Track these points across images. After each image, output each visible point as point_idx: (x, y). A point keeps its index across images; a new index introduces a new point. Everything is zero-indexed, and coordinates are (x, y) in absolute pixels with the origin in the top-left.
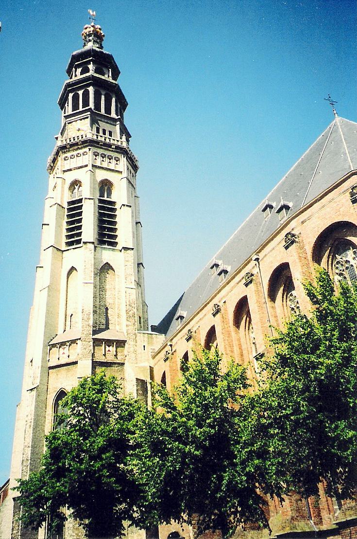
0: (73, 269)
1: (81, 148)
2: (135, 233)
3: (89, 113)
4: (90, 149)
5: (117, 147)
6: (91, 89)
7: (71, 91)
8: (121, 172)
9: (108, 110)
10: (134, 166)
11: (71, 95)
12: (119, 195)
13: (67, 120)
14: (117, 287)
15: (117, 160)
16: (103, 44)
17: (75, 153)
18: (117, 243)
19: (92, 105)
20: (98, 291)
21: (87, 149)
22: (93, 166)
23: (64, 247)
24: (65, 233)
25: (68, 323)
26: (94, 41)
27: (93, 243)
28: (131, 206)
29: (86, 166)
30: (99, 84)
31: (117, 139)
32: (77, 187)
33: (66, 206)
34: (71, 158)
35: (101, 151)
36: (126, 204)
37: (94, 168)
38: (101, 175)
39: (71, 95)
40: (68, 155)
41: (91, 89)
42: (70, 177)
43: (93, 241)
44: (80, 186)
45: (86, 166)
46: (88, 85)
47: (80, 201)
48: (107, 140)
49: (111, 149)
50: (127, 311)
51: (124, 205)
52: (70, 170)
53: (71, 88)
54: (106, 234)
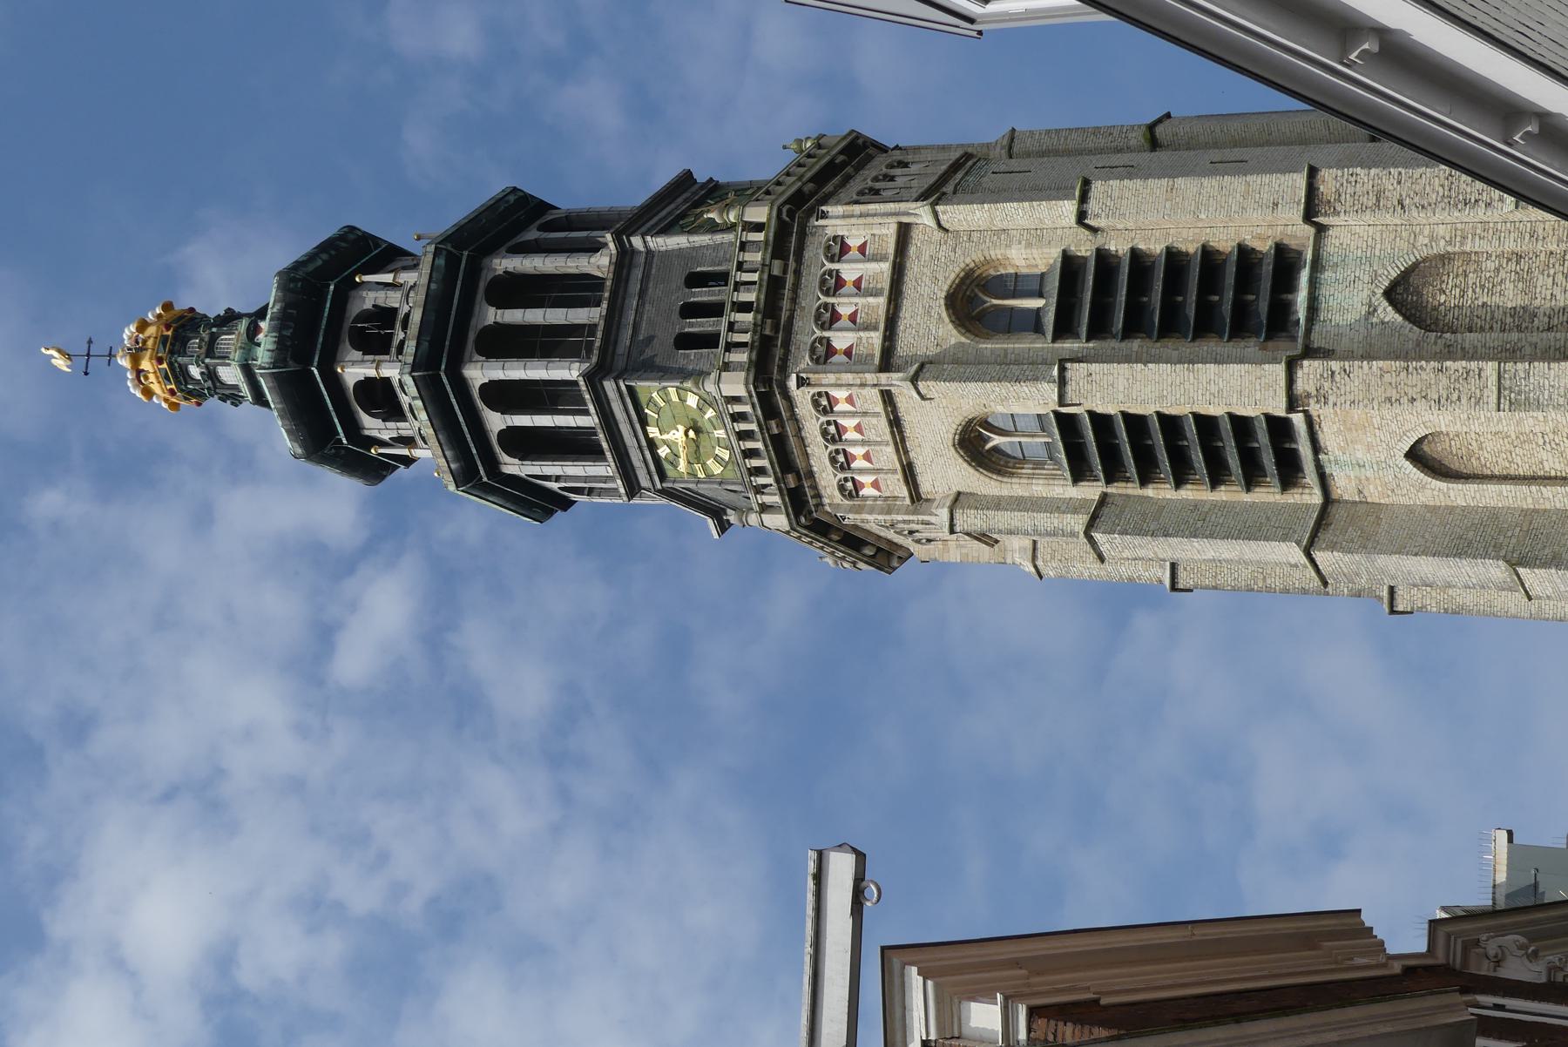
0: (1415, 455)
2: (1216, 155)
3: (609, 386)
4: (801, 382)
5: (779, 248)
6: (479, 374)
7: (493, 465)
8: (904, 232)
9: (578, 290)
10: (847, 164)
11: (512, 466)
12: (1028, 236)
13: (644, 482)
14: (1510, 245)
15: (838, 250)
16: (215, 310)
19: (568, 371)
20: (1535, 338)
21: (802, 398)
22: (886, 365)
26: (210, 353)
27: (1291, 367)
28: (1086, 183)
29: (888, 398)
31: (734, 240)
32: (997, 440)
33: (1091, 491)
34: (846, 467)
35: (806, 332)
36: (1069, 208)
37: (896, 361)
38: (928, 326)
39: (512, 466)
42: (945, 472)
44: (986, 424)
45: (888, 398)
46: (461, 385)
47: (1067, 424)
48: (749, 296)
49: (790, 278)
51: (1081, 217)
52: (909, 474)
53: (475, 468)
54: (1240, 299)
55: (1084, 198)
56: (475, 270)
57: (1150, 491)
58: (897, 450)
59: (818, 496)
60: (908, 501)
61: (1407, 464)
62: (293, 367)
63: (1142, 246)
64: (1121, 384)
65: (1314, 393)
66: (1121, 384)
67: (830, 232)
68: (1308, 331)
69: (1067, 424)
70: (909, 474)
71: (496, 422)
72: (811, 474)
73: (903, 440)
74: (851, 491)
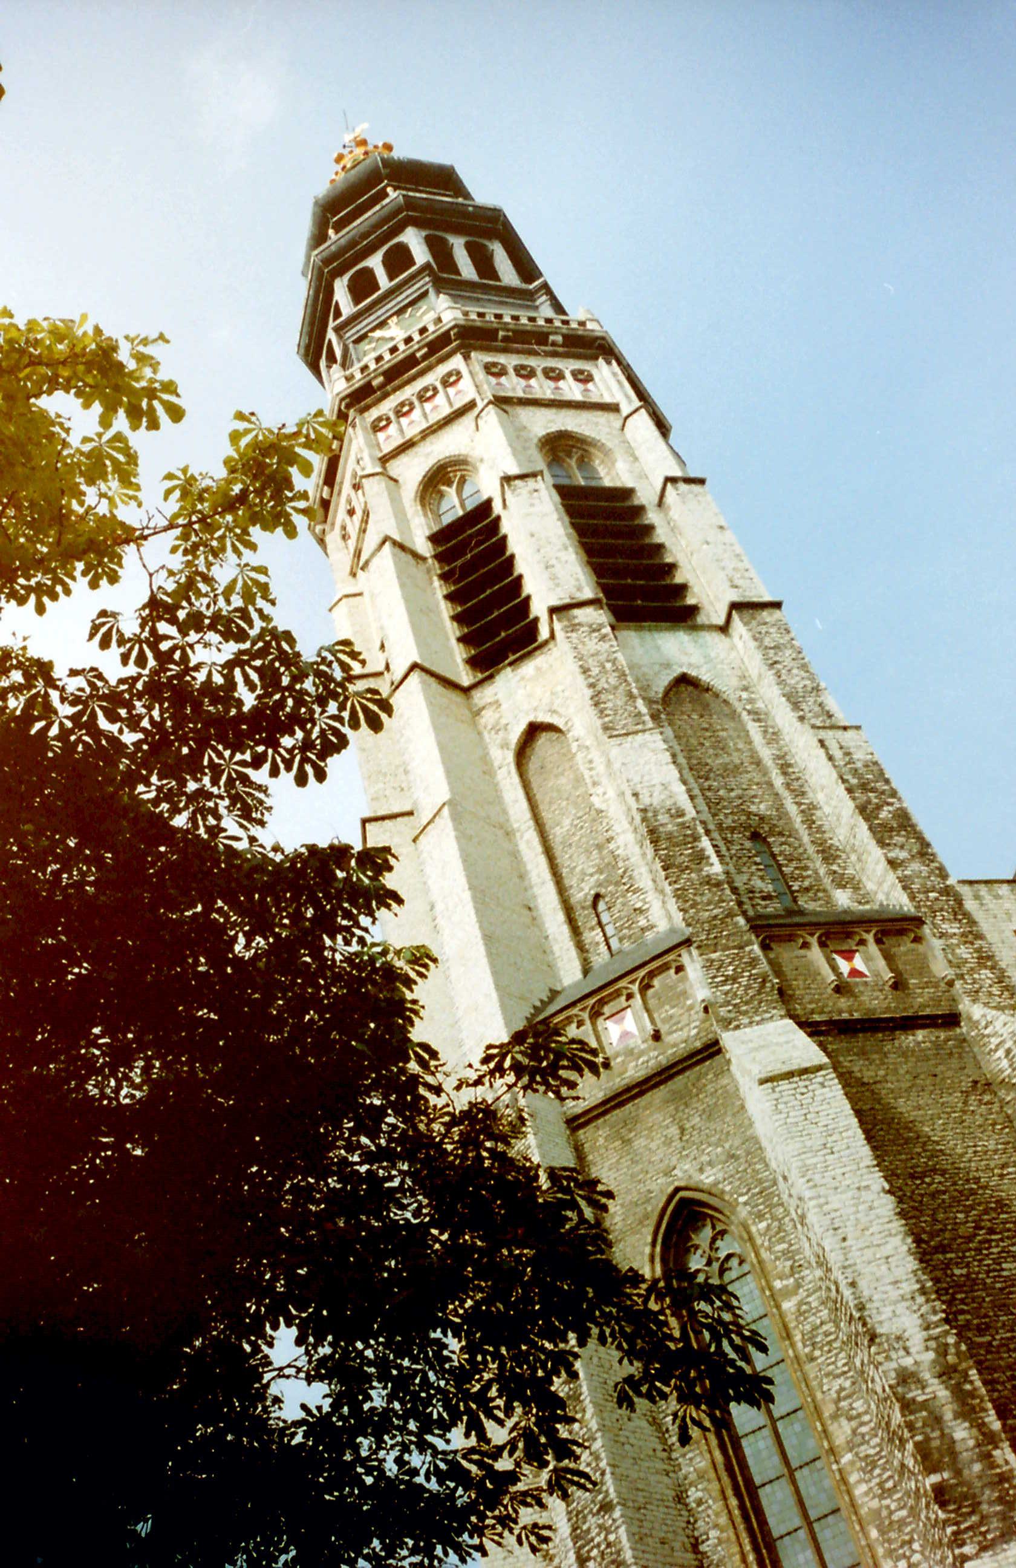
4: (467, 357)
7: (339, 272)
8: (614, 408)
23: (466, 677)
24: (453, 631)
25: (593, 936)
35: (509, 361)
40: (387, 407)
41: (413, 240)
44: (463, 481)
46: (399, 229)
52: (407, 446)
57: (437, 583)
58: (423, 431)
60: (380, 455)
65: (576, 621)
67: (595, 372)
70: (407, 446)
72: (386, 395)
73: (434, 432)
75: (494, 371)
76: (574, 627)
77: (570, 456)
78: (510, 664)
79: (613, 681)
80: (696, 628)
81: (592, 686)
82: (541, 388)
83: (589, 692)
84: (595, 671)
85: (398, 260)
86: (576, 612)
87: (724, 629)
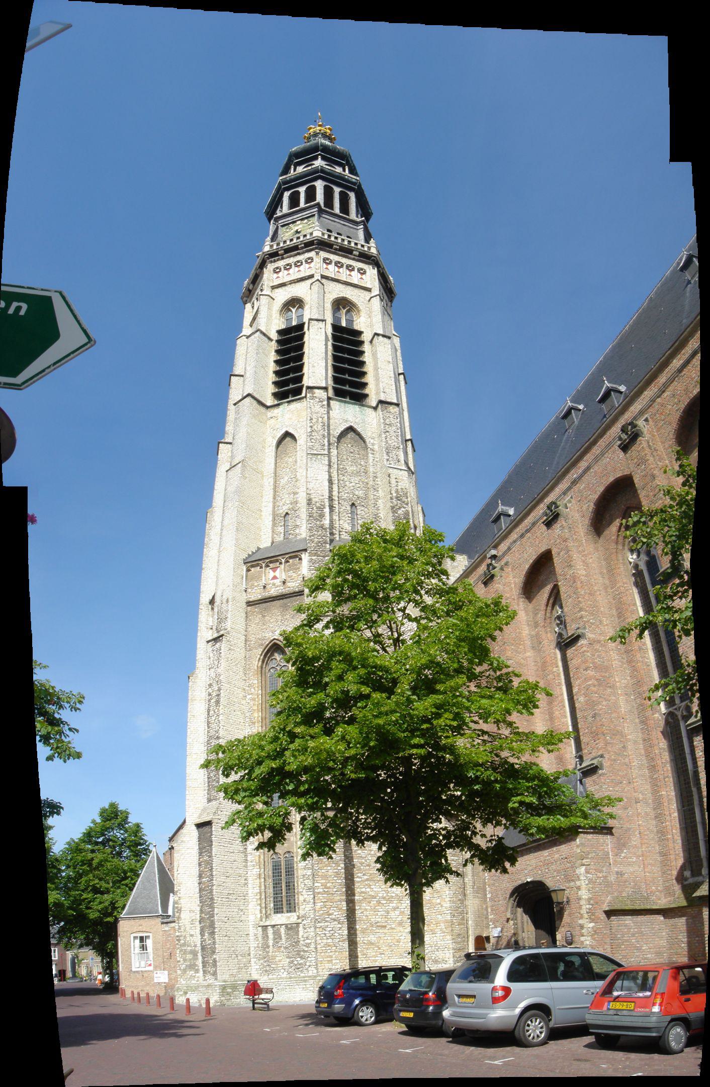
1: (303, 253)
4: (317, 253)
6: (319, 185)
7: (287, 189)
8: (369, 290)
11: (287, 195)
14: (371, 469)
17: (292, 260)
18: (366, 396)
21: (312, 254)
23: (270, 401)
24: (272, 377)
27: (325, 389)
30: (331, 179)
33: (274, 336)
35: (334, 258)
36: (381, 332)
38: (336, 291)
39: (287, 195)
41: (319, 185)
42: (283, 296)
43: (324, 385)
45: (312, 276)
46: (315, 179)
50: (393, 508)
51: (376, 334)
52: (283, 285)
55: (384, 336)
56: (351, 189)
57: (273, 353)
59: (275, 261)
61: (283, 432)
62: (321, 148)
63: (366, 354)
64: (317, 337)
66: (317, 337)
67: (368, 271)
68: (337, 400)
69: (300, 327)
70: (283, 285)
71: (302, 190)
72: (283, 259)
74: (277, 271)
75: (326, 261)
76: (313, 398)
77: (344, 308)
78: (288, 402)
79: (320, 427)
80: (363, 405)
81: (311, 427)
82: (344, 274)
83: (309, 429)
84: (314, 420)
85: (311, 195)
86: (316, 391)
87: (375, 408)
